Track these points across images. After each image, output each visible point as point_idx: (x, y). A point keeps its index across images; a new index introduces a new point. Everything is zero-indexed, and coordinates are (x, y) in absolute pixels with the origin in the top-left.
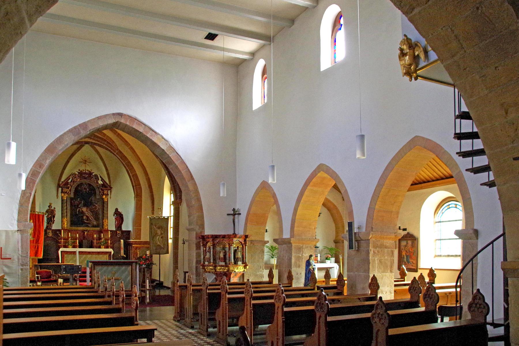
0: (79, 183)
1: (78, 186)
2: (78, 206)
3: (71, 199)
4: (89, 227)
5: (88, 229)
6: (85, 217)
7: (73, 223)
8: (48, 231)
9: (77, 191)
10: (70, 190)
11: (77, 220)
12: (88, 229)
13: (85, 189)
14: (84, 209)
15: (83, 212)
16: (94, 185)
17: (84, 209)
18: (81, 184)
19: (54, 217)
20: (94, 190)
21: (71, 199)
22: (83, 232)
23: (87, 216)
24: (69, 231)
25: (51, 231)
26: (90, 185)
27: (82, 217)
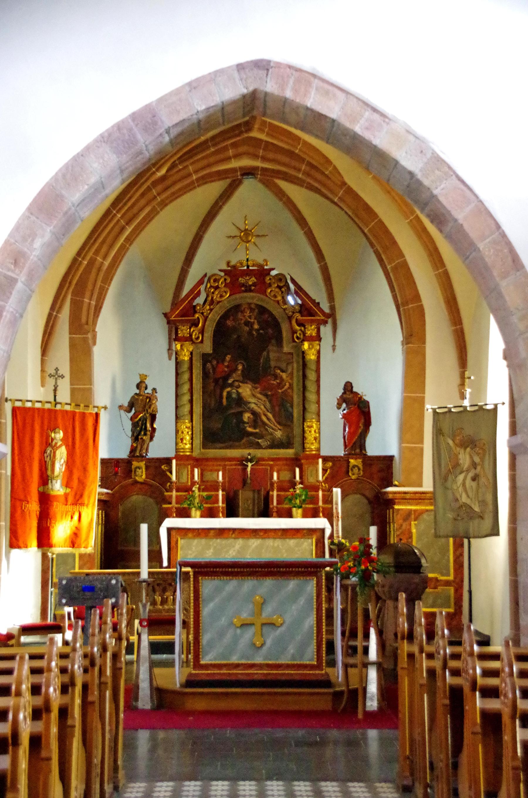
0: (228, 306)
1: (225, 317)
2: (226, 378)
3: (205, 358)
4: (258, 446)
5: (258, 453)
6: (247, 416)
7: (210, 438)
8: (135, 464)
9: (221, 332)
10: (202, 332)
11: (221, 425)
12: (258, 453)
13: (247, 323)
14: (246, 391)
15: (240, 401)
16: (276, 312)
17: (246, 391)
18: (236, 309)
19: (153, 418)
20: (277, 326)
21: (205, 358)
22: (242, 462)
23: (254, 413)
24: (198, 462)
25: (143, 464)
26: (262, 310)
27: (241, 414)
